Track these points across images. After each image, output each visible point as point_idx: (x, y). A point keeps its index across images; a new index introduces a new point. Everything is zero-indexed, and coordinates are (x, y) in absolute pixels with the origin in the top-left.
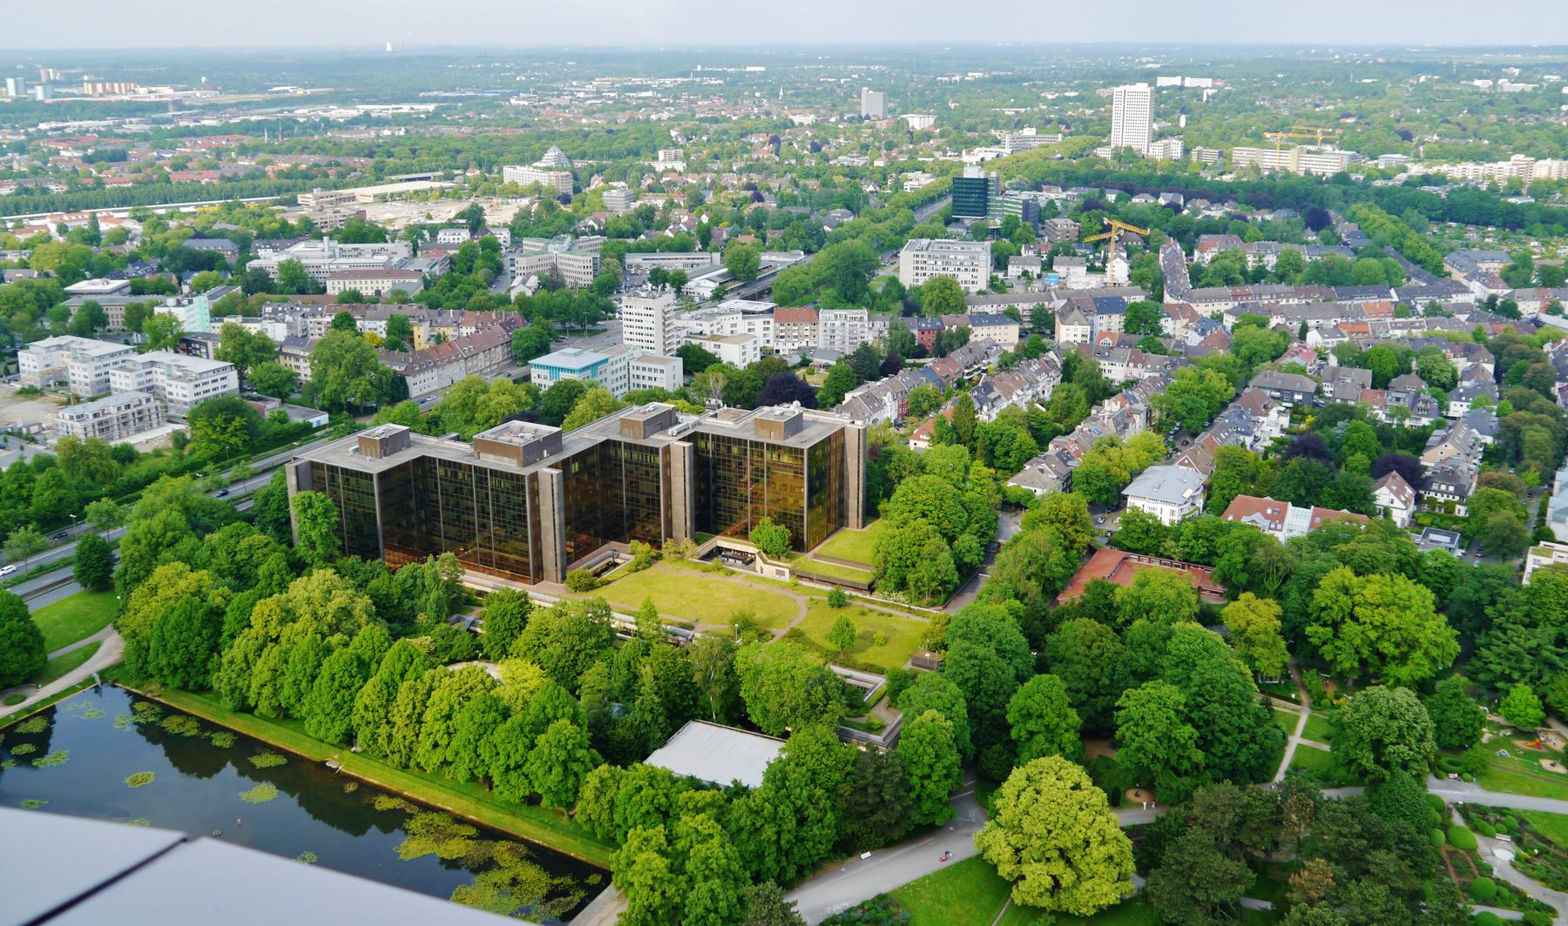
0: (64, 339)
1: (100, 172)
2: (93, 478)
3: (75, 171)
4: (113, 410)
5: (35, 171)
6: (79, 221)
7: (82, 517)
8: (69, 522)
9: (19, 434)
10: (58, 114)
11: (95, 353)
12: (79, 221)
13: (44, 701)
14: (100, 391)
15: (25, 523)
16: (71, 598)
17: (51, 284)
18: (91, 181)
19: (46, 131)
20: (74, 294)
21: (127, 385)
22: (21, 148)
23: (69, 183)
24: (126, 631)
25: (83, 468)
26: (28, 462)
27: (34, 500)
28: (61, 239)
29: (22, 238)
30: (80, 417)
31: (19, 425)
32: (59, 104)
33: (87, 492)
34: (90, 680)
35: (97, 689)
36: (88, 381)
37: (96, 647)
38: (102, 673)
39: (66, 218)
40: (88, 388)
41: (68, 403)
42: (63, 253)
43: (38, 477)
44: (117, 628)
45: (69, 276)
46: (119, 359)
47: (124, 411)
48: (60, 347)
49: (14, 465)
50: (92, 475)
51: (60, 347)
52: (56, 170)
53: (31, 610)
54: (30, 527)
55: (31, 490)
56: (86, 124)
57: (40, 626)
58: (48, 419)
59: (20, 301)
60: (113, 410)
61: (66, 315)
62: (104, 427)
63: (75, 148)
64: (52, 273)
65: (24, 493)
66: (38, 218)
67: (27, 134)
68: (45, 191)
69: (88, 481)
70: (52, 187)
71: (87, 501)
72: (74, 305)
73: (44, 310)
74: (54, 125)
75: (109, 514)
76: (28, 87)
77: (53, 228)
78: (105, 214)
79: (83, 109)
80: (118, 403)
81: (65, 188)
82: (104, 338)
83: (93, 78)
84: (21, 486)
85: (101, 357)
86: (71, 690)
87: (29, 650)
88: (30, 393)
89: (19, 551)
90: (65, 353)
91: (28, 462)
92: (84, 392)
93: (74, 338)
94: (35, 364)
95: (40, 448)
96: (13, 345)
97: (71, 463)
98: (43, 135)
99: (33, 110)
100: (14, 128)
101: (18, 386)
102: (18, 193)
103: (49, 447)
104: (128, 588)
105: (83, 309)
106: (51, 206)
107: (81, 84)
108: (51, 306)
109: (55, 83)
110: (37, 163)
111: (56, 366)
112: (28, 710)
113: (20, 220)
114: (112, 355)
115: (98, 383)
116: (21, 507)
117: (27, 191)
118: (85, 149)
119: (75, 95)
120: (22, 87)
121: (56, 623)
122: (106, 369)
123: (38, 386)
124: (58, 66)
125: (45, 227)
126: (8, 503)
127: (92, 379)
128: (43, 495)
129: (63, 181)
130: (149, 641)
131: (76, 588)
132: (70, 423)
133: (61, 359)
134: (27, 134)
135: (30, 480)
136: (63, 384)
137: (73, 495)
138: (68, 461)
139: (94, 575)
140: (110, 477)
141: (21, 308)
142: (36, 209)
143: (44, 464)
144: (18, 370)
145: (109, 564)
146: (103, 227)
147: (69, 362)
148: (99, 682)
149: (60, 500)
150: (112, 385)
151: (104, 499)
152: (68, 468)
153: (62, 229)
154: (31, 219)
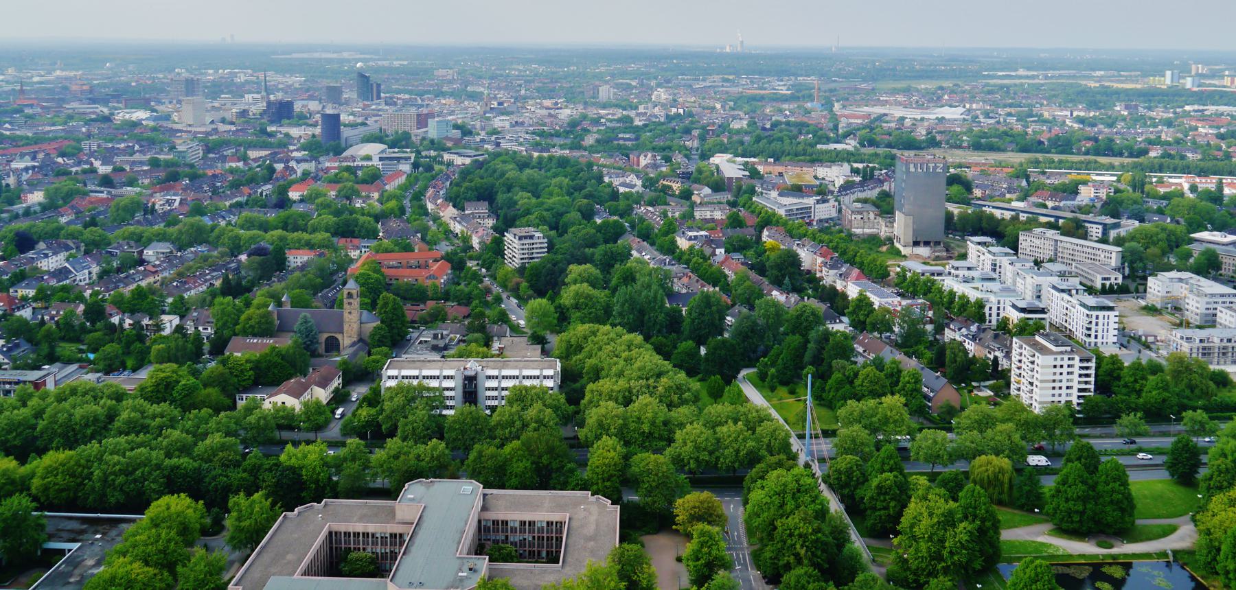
0: (1185, 275)
1: (1229, 147)
2: (1192, 391)
3: (1208, 144)
4: (1217, 340)
5: (1178, 142)
6: (1208, 183)
7: (1179, 420)
8: (1168, 420)
9: (1138, 339)
10: (1201, 99)
11: (1208, 291)
12: (1208, 183)
13: (1126, 555)
14: (1206, 321)
15: (1135, 410)
16: (1160, 482)
17: (1181, 229)
18: (1221, 153)
19: (1190, 112)
20: (1196, 240)
21: (1230, 322)
22: (1169, 123)
23: (1203, 153)
24: (1202, 527)
25: (1186, 381)
26: (1144, 362)
27: (1144, 394)
28: (1191, 195)
29: (1162, 190)
30: (1189, 339)
31: (1140, 333)
32: (1202, 92)
33: (1185, 401)
34: (1163, 554)
35: (1168, 564)
36: (1198, 311)
37: (1173, 529)
38: (1175, 552)
39: (1197, 180)
40: (1198, 318)
41: (1180, 325)
42: (1192, 207)
43: (1151, 378)
44: (1194, 520)
45: (1195, 226)
46: (1228, 300)
47: (1225, 343)
48: (1181, 280)
49: (1134, 363)
50: (1192, 388)
51: (1181, 280)
52: (1194, 143)
53: (1131, 480)
54: (1139, 415)
55: (1143, 386)
56: (1222, 108)
57: (1133, 494)
58: (1163, 334)
59: (1155, 238)
60: (1217, 340)
61: (1189, 255)
62: (1207, 352)
63: (1211, 127)
64: (1182, 221)
65: (1137, 386)
66: (1175, 177)
67: (1175, 113)
68: (1183, 157)
69: (1188, 392)
70: (1189, 155)
71: (1185, 408)
72: (1196, 249)
73: (1172, 249)
74: (1196, 107)
75: (1202, 424)
76: (1180, 78)
77: (1186, 187)
78: (1229, 181)
79: (1221, 97)
80: (1222, 336)
81: (1199, 157)
82: (1215, 279)
83: (1232, 73)
84: (1136, 381)
85: (1213, 295)
86: (1148, 555)
87: (1123, 510)
88: (1152, 310)
89: (1127, 430)
90: (1184, 286)
91: (1144, 362)
92: (1195, 319)
93: (1193, 275)
94: (1160, 289)
95: (1153, 355)
96: (1144, 271)
97: (1177, 374)
98: (1187, 114)
99: (1181, 96)
100: (1165, 107)
101: (1143, 303)
102: (1163, 157)
103: (1161, 356)
104: (1211, 490)
105: (1203, 253)
106: (1186, 170)
107: (1222, 77)
108: (1177, 247)
109: (1202, 76)
110: (1180, 135)
111: (1175, 294)
112: (1114, 557)
113: (1162, 177)
114: (1222, 295)
115: (1207, 315)
116: (1134, 396)
117: (1170, 156)
118: (1218, 128)
119: (1216, 86)
120: (1176, 77)
121: (1145, 497)
122: (1215, 306)
123: (1159, 306)
124: (1205, 63)
125: (1180, 184)
126: (1124, 390)
127: (1202, 310)
128: (1151, 392)
129: (1199, 151)
130: (1220, 543)
131: (1164, 474)
132: (1180, 341)
133: (1180, 290)
134: (1175, 113)
135: (1144, 378)
136: (1177, 309)
137: (1174, 400)
138: (1175, 371)
139: (1181, 470)
140: (1206, 394)
141: (1155, 244)
142: (1175, 170)
143: (1155, 369)
144: (1145, 291)
145: (1197, 464)
146: (1227, 191)
147: (1186, 292)
148: (1171, 559)
149: (1164, 401)
150: (1218, 320)
151: (1199, 411)
152: (1174, 377)
153: (1193, 188)
154: (1170, 177)
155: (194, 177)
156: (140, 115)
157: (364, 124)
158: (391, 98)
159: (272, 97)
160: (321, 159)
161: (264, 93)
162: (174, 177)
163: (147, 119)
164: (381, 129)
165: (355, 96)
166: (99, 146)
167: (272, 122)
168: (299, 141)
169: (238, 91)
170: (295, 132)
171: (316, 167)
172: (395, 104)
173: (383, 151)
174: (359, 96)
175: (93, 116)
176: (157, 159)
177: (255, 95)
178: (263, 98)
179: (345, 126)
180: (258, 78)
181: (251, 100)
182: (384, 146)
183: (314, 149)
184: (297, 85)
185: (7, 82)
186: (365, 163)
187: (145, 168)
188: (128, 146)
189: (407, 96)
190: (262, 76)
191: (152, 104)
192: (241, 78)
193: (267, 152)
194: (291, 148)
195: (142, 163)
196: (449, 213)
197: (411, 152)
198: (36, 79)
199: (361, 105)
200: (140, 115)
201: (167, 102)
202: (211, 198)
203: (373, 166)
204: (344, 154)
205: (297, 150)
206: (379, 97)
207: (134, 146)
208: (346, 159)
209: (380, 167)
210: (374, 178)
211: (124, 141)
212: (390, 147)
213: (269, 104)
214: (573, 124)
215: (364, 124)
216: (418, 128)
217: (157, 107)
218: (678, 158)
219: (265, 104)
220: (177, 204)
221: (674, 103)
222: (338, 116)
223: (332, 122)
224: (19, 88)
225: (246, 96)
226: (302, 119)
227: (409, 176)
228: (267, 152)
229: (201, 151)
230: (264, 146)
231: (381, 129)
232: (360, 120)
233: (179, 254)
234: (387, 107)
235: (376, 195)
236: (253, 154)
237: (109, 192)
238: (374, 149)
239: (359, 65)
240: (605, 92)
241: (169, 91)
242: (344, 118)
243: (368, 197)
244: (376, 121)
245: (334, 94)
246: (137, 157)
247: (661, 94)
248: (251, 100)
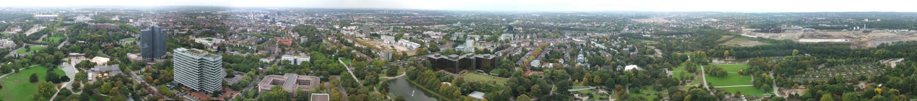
162: (251, 26)
170: (268, 20)
183: (271, 23)
196: (292, 33)
210: (280, 28)
214: (312, 20)
218: (328, 25)
221: (328, 16)
222: (274, 18)
223: (274, 19)
226: (269, 18)
236: (262, 23)
240: (317, 15)
245: (274, 15)
247: (326, 15)
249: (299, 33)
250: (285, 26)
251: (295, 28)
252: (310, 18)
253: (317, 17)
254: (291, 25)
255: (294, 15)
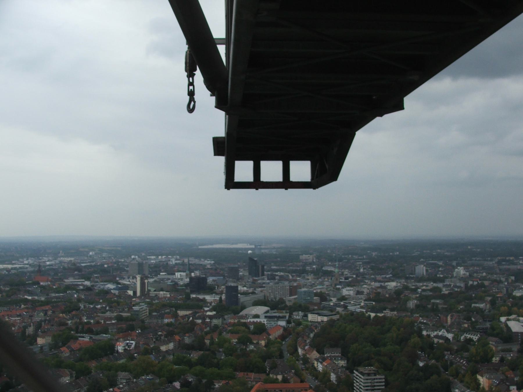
155: (144, 328)
156: (111, 286)
157: (253, 293)
158: (272, 275)
159: (193, 274)
160: (226, 317)
161: (188, 272)
163: (114, 289)
164: (265, 296)
165: (247, 274)
166: (85, 307)
167: (192, 292)
168: (211, 304)
169: (171, 271)
171: (223, 323)
172: (274, 279)
173: (267, 312)
174: (250, 274)
175: (81, 287)
176: (121, 315)
177: (182, 273)
178: (187, 275)
179: (242, 294)
180: (183, 261)
181: (179, 277)
182: (266, 308)
184: (209, 267)
185: (30, 265)
186: (255, 320)
187: (113, 322)
188: (103, 307)
189: (282, 274)
190: (186, 260)
191: (117, 279)
192: (173, 261)
193: (190, 312)
194: (206, 309)
195: (110, 319)
197: (286, 313)
198: (48, 263)
199: (251, 280)
200: (111, 286)
201: (126, 277)
202: (155, 342)
203: (260, 322)
204: (241, 314)
205: (210, 311)
206: (263, 275)
207: (106, 307)
208: (243, 317)
209: (265, 322)
210: (261, 329)
211: (100, 304)
212: (272, 309)
213: (191, 279)
215: (253, 293)
216: (290, 296)
217: (120, 281)
219: (188, 280)
220: (133, 346)
222: (237, 287)
223: (232, 292)
224: (36, 269)
225: (176, 274)
227: (285, 329)
228: (190, 312)
229: (148, 311)
230: (187, 308)
231: (265, 296)
232: (251, 290)
233: (135, 380)
234: (268, 281)
235: (263, 343)
236: (181, 313)
237: (91, 338)
238: (260, 310)
239: (250, 252)
241: (127, 271)
242: (240, 288)
243: (258, 343)
244: (261, 291)
245: (234, 273)
246: (108, 314)
248: (179, 277)
249: (344, 355)
250: (283, 323)
251: (326, 328)
252: (392, 285)
253: (421, 279)
254: (311, 317)
255: (320, 273)
